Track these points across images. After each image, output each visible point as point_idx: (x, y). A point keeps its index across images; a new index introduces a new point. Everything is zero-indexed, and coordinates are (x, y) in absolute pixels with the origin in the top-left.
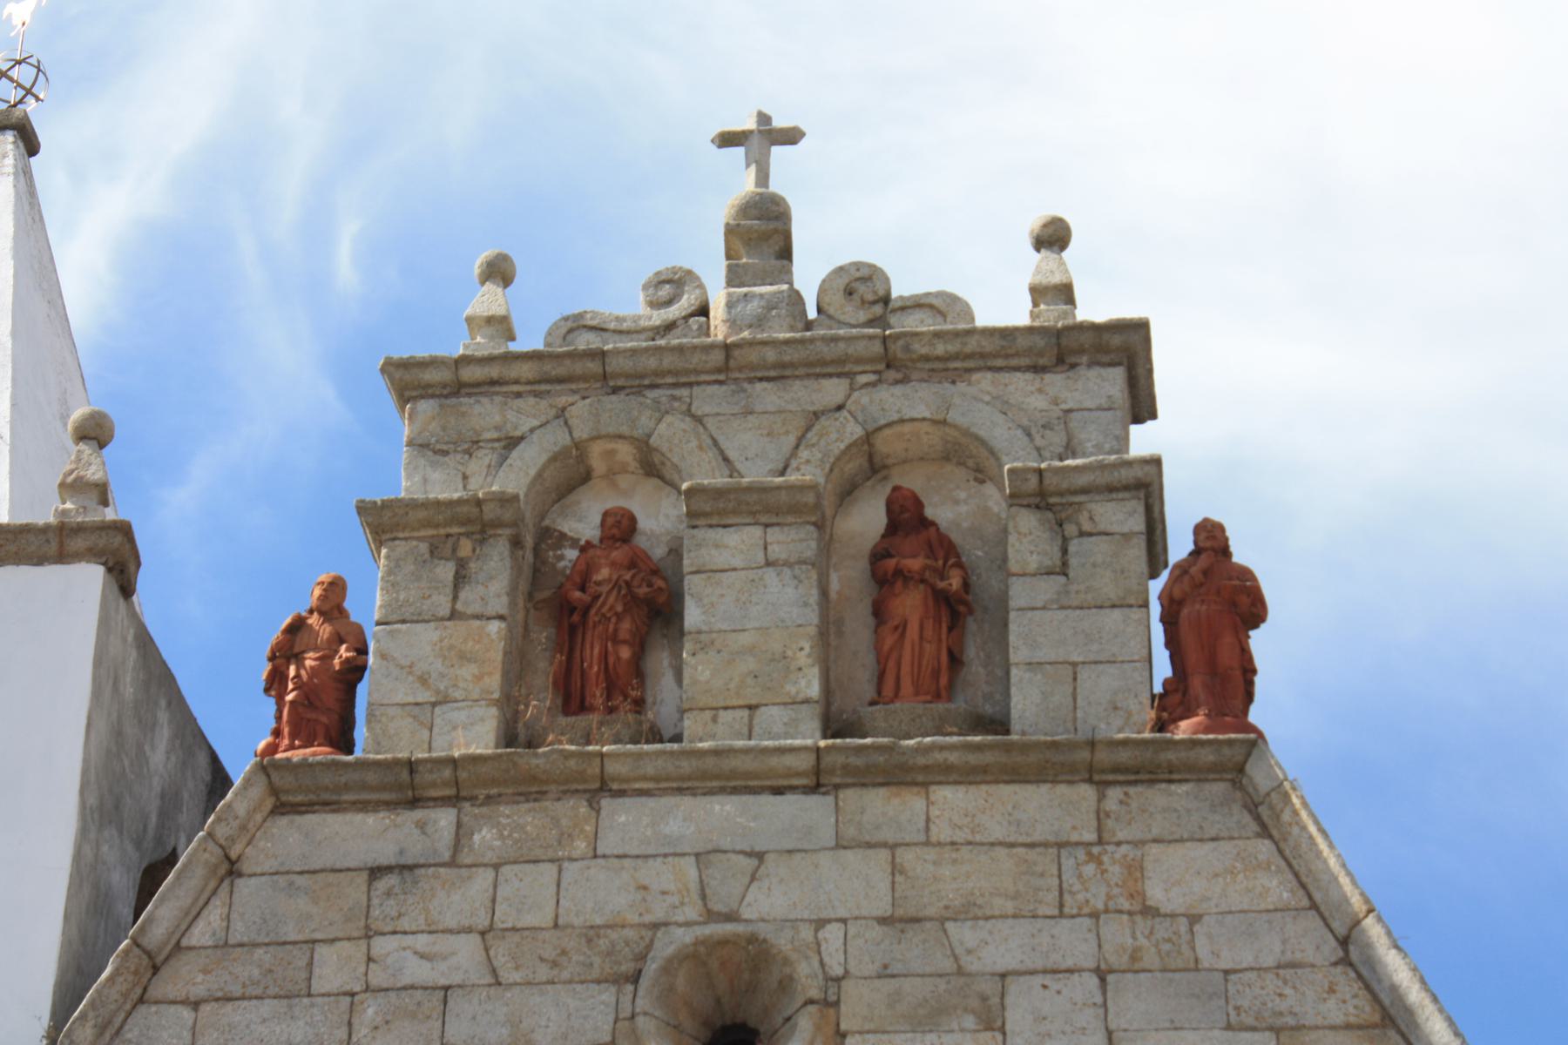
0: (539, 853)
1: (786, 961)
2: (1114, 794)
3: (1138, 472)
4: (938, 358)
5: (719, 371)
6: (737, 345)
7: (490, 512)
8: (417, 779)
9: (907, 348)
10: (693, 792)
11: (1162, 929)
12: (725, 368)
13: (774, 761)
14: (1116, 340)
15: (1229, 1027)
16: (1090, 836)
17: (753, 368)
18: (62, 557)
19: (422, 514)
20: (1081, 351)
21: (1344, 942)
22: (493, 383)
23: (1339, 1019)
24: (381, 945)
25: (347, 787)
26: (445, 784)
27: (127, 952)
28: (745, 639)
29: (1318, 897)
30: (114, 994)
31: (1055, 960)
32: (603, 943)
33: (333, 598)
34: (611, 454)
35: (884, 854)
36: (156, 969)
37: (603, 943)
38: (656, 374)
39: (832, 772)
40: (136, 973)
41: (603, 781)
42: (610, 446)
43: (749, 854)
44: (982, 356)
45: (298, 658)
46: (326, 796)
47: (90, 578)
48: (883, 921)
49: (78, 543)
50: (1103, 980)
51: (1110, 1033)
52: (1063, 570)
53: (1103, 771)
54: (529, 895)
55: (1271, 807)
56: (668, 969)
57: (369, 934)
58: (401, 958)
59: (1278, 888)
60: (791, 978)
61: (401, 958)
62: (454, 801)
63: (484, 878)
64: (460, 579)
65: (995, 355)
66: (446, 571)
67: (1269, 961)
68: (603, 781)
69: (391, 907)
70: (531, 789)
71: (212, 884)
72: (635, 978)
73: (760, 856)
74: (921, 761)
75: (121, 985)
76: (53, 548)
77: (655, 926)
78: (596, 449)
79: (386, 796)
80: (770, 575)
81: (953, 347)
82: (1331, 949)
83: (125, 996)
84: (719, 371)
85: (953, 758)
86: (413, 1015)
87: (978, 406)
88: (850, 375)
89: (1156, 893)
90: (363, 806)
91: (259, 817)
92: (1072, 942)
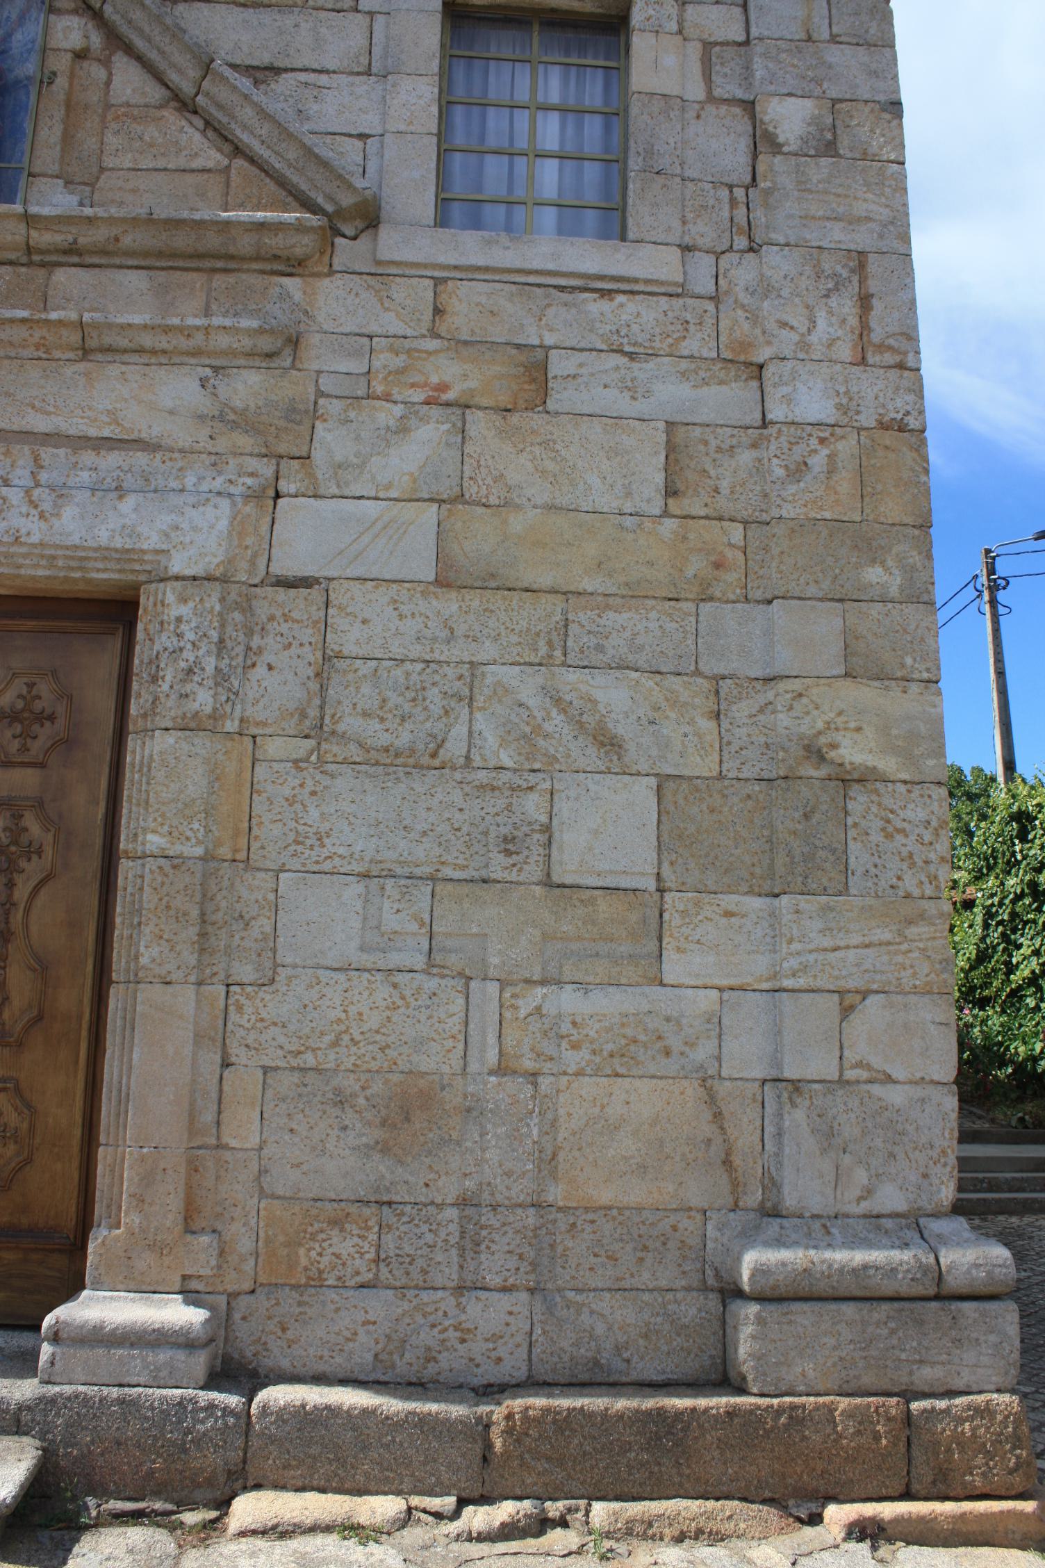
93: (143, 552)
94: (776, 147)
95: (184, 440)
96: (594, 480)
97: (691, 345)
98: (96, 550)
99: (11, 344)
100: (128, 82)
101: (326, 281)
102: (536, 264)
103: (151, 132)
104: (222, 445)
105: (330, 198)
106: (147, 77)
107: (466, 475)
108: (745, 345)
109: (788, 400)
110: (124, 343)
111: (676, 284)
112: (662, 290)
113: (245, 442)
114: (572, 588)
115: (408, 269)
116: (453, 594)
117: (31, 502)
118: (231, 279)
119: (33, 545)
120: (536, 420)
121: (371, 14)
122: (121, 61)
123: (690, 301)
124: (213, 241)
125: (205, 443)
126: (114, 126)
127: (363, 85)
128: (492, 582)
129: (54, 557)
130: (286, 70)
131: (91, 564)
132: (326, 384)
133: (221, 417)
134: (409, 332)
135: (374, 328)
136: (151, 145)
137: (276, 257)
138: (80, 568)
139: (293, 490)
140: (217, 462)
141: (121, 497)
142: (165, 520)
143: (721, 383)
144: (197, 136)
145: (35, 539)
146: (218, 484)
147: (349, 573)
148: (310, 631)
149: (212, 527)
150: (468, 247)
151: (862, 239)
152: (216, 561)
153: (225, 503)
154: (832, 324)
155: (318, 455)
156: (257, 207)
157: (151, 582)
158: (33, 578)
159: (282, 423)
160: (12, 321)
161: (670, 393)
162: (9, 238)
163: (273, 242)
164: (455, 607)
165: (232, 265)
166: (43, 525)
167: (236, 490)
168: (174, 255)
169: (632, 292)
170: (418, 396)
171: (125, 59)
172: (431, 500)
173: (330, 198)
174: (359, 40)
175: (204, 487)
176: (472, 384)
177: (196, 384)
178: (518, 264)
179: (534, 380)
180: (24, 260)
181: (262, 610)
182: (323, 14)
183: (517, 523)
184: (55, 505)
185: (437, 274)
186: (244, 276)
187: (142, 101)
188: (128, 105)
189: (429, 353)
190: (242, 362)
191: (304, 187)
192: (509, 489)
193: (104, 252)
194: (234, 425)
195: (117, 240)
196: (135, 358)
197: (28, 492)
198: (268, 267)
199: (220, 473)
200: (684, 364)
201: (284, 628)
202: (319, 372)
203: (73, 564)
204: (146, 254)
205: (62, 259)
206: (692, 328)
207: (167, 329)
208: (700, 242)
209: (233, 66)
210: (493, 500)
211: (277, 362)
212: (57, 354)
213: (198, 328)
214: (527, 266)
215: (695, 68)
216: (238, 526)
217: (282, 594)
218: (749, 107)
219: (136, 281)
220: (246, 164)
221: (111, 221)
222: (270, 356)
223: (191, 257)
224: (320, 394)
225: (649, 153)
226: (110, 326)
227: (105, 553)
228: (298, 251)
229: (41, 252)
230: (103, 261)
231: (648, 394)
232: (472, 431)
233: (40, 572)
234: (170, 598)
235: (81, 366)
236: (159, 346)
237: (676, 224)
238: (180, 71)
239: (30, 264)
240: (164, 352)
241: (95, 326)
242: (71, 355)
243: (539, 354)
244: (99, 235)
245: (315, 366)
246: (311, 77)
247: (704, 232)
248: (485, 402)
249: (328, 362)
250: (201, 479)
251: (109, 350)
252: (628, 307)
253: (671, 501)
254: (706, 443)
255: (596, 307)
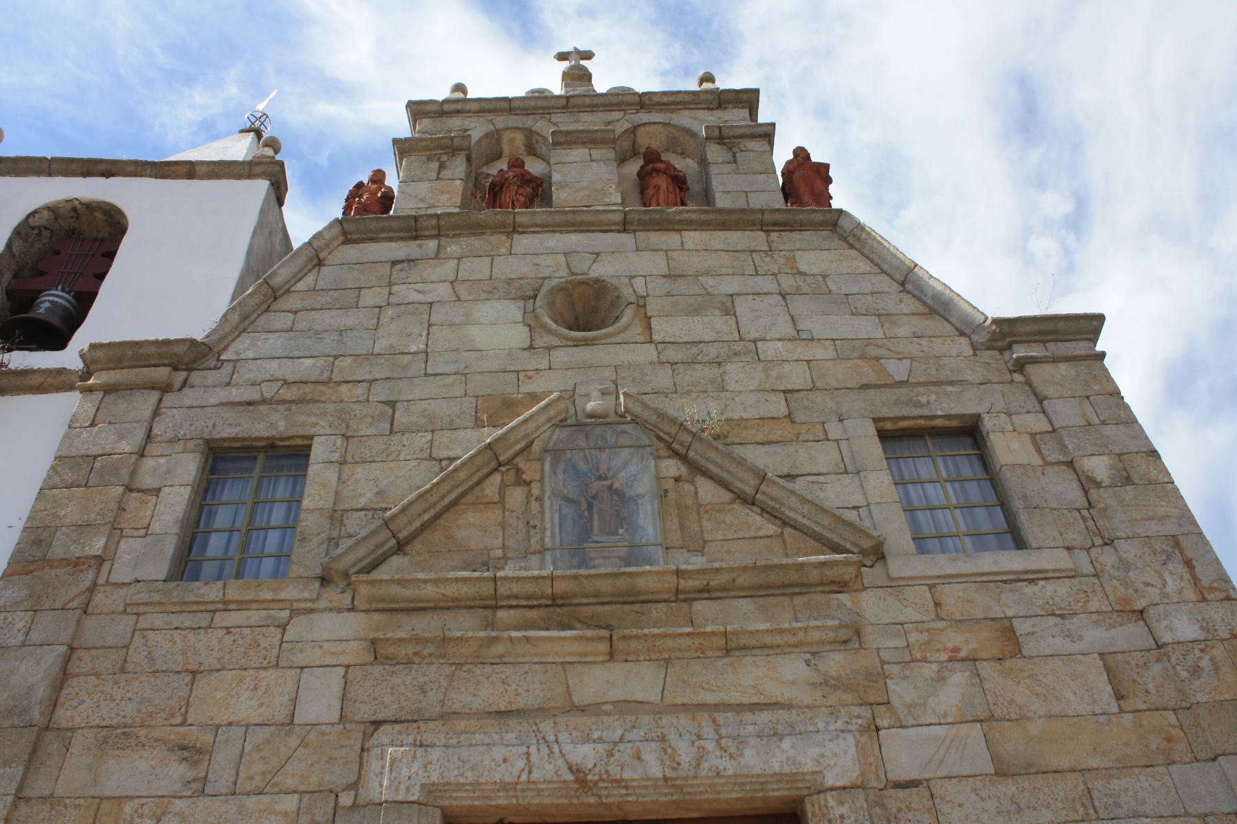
0: (481, 253)
1: (616, 289)
2: (774, 236)
3: (765, 129)
4: (664, 104)
5: (563, 108)
6: (572, 96)
7: (457, 142)
8: (419, 225)
9: (650, 99)
10: (561, 232)
11: (810, 280)
12: (566, 107)
13: (603, 217)
14: (745, 97)
15: (853, 314)
16: (765, 248)
17: (579, 107)
18: (250, 176)
19: (424, 144)
20: (729, 102)
21: (903, 284)
22: (458, 112)
23: (908, 311)
24: (395, 289)
25: (382, 230)
26: (433, 228)
27: (261, 285)
28: (584, 184)
29: (885, 267)
30: (252, 302)
31: (757, 290)
32: (516, 285)
33: (378, 177)
34: (512, 140)
35: (662, 253)
36: (276, 299)
37: (516, 285)
38: (534, 108)
39: (632, 223)
40: (265, 296)
41: (514, 228)
42: (513, 135)
43: (593, 253)
44: (684, 103)
45: (360, 196)
46: (371, 235)
47: (261, 187)
48: (664, 276)
49: (258, 170)
50: (784, 298)
51: (792, 317)
52: (735, 161)
53: (767, 225)
54: (478, 268)
55: (854, 236)
56: (551, 292)
57: (390, 285)
58: (407, 293)
59: (864, 266)
60: (619, 297)
61: (407, 293)
62: (438, 236)
63: (452, 264)
64: (442, 167)
65: (689, 103)
66: (435, 165)
67: (867, 291)
68: (514, 228)
69: (403, 275)
70: (477, 229)
71: (309, 267)
72: (535, 297)
73: (598, 254)
74: (678, 217)
75: (256, 300)
76: (246, 171)
77: (544, 278)
78: (506, 136)
79: (402, 235)
80: (594, 164)
81: (671, 99)
82: (895, 287)
83: (259, 305)
84: (563, 108)
85: (694, 216)
86: (413, 313)
87: (684, 119)
88: (625, 110)
89: (803, 267)
90: (390, 239)
91: (336, 244)
92: (767, 284)
93: (804, 774)
94: (1098, 485)
95: (807, 700)
96: (1069, 695)
97: (1094, 605)
98: (772, 776)
99: (680, 650)
100: (708, 491)
101: (863, 594)
102: (986, 569)
103: (729, 518)
104: (832, 700)
105: (856, 545)
106: (719, 488)
107: (991, 702)
108: (1126, 601)
109: (1169, 628)
110: (753, 643)
111: (1071, 570)
112: (1063, 574)
113: (847, 697)
114: (1083, 767)
115: (911, 581)
116: (1010, 781)
117: (722, 748)
118: (805, 598)
119: (729, 777)
120: (1020, 663)
121: (837, 441)
122: (700, 480)
123: (1083, 579)
124: (793, 576)
125: (820, 701)
126: (705, 516)
127: (847, 480)
128: (1032, 770)
129: (743, 784)
130: (798, 476)
131: (769, 786)
132: (885, 655)
133: (826, 683)
134: (924, 619)
135: (902, 619)
136: (732, 525)
137: (832, 582)
138: (762, 790)
139: (886, 724)
140: (833, 712)
141: (780, 740)
142: (814, 752)
143: (1121, 625)
144: (758, 518)
145: (730, 772)
146: (840, 724)
147: (940, 773)
148: (927, 816)
149: (846, 752)
150: (942, 564)
151: (1170, 528)
152: (855, 774)
153: (849, 737)
154: (1174, 579)
155: (895, 700)
156: (806, 554)
157: (811, 795)
158: (727, 801)
159: (866, 683)
160: (681, 635)
161: (1095, 636)
162: (667, 585)
163: (832, 573)
164: (1013, 789)
165: (805, 590)
166: (734, 763)
167: (854, 728)
168: (769, 587)
169: (1046, 579)
170: (944, 657)
171: (703, 479)
172: (974, 721)
173: (856, 545)
174: (834, 455)
175: (831, 728)
176: (972, 646)
177: (804, 665)
178: (975, 570)
179: (1009, 639)
180: (673, 598)
181: (892, 805)
182: (810, 444)
183: (1034, 728)
184: (738, 748)
185: (928, 582)
186: (812, 596)
187: (719, 501)
188: (711, 504)
189: (941, 630)
190: (828, 647)
191: (836, 539)
192: (1020, 708)
193: (725, 589)
194: (836, 688)
195: (734, 581)
196: (759, 652)
197: (717, 742)
198: (827, 589)
199: (837, 718)
200: (1095, 617)
201: (910, 815)
202: (878, 649)
203: (757, 787)
204: (751, 588)
205: (698, 595)
206: (1091, 595)
207: (781, 631)
208: (1074, 543)
209: (780, 477)
210: (1013, 716)
211: (850, 646)
212: (710, 653)
213: (800, 629)
214: (981, 571)
215: (1031, 448)
216: (862, 753)
217: (901, 793)
218: (1070, 464)
219: (745, 605)
220: (793, 531)
221: (731, 569)
222: (845, 642)
223: (778, 587)
224: (883, 662)
225: (1025, 497)
226: (744, 632)
227: (779, 777)
228: (846, 577)
229: (684, 592)
230: (724, 594)
231: (1081, 638)
232: (984, 674)
233: (734, 795)
234: (831, 803)
235: (727, 660)
236: (775, 643)
237: (1058, 535)
238: (743, 482)
239: (677, 600)
240: (778, 646)
241: (735, 633)
242: (719, 653)
243: (1006, 622)
244: (723, 578)
245: (874, 646)
246: (815, 478)
247: (1075, 536)
248: (985, 655)
249: (884, 643)
250: (827, 723)
251: (744, 648)
252: (1049, 588)
253: (1121, 702)
254: (1128, 663)
255: (1030, 590)
